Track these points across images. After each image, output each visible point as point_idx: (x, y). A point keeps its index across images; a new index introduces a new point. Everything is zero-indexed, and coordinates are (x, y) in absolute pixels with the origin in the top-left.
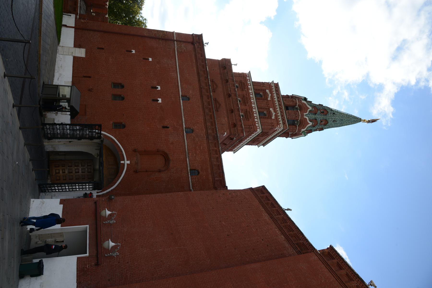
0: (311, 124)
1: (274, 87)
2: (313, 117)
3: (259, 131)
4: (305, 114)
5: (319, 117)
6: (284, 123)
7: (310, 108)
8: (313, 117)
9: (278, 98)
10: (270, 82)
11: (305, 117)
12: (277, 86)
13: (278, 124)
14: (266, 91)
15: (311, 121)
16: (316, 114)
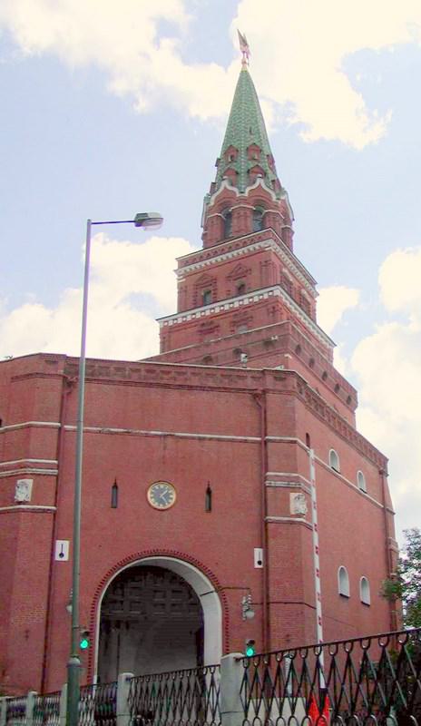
0: (259, 181)
1: (187, 268)
2: (243, 179)
3: (278, 291)
4: (238, 195)
5: (243, 164)
6: (260, 239)
7: (225, 184)
8: (243, 179)
9: (209, 257)
10: (176, 276)
11: (246, 194)
12: (184, 262)
13: (262, 251)
14: (198, 284)
16: (237, 173)
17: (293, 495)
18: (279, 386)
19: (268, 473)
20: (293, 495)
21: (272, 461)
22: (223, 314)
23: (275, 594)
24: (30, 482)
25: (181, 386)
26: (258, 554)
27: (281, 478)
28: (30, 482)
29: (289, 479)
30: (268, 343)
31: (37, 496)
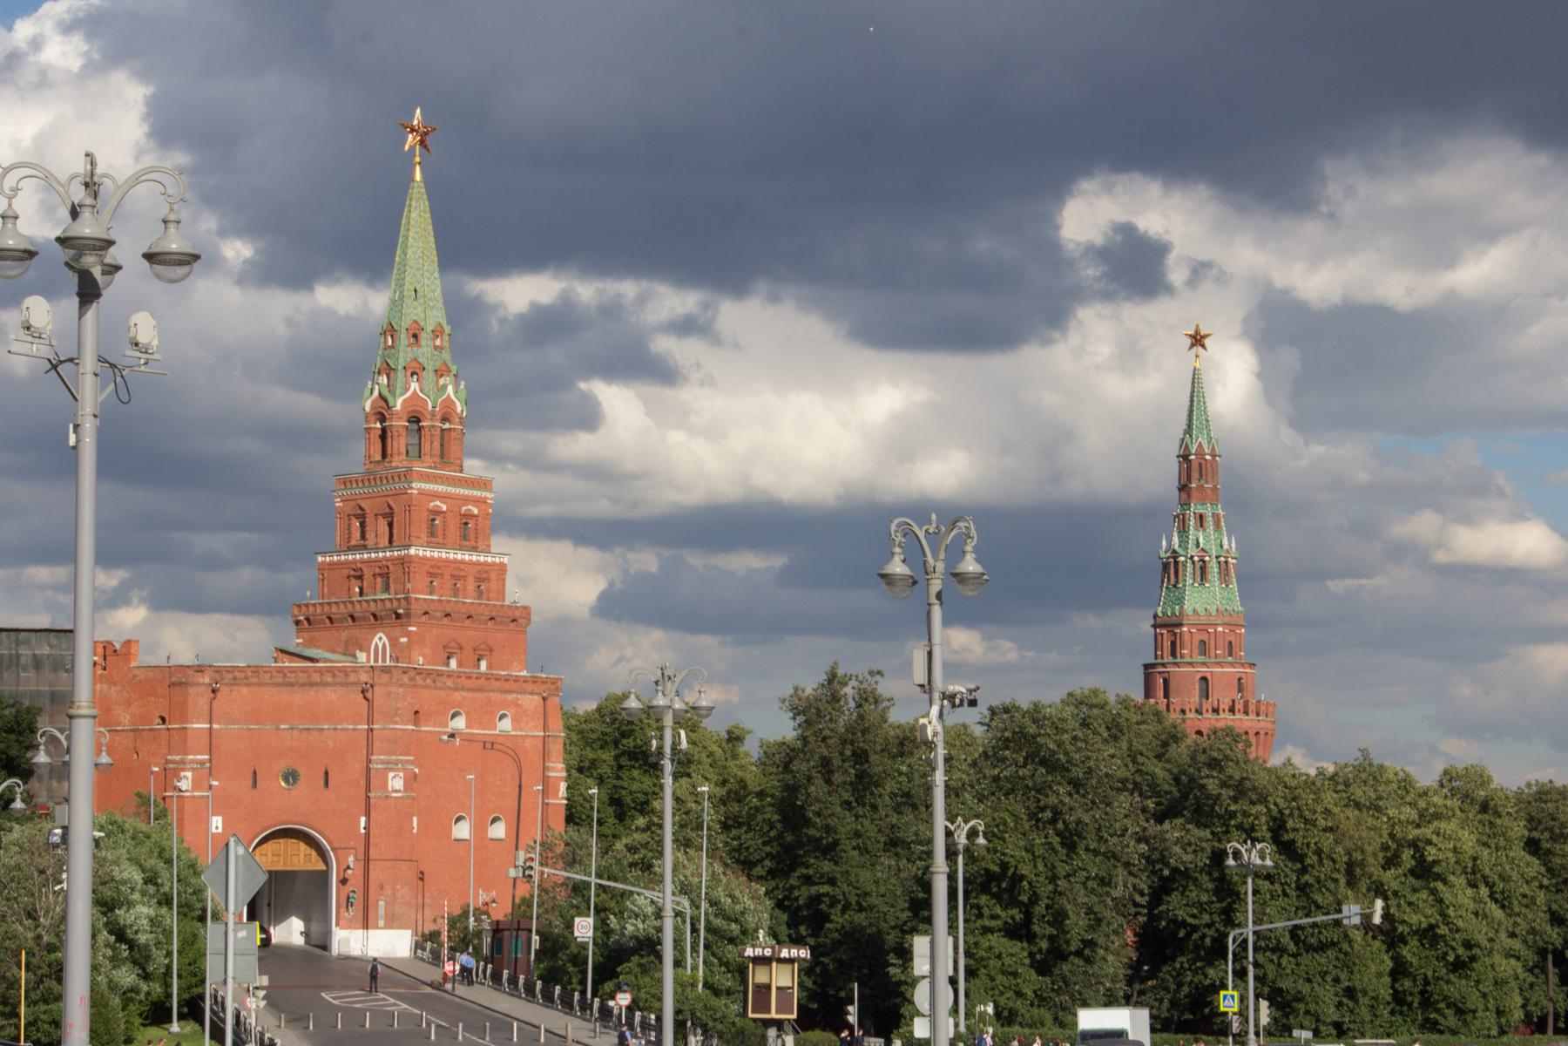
0: (414, 386)
11: (398, 407)
15: (407, 390)
17: (391, 775)
18: (385, 677)
19: (374, 757)
20: (391, 775)
21: (377, 744)
22: (370, 561)
23: (373, 854)
24: (189, 774)
25: (303, 685)
26: (363, 820)
27: (383, 762)
28: (189, 774)
29: (389, 762)
30: (398, 616)
31: (195, 786)
